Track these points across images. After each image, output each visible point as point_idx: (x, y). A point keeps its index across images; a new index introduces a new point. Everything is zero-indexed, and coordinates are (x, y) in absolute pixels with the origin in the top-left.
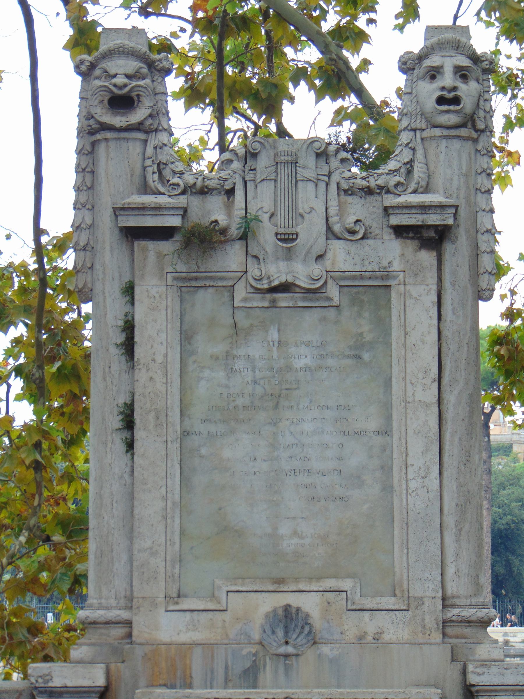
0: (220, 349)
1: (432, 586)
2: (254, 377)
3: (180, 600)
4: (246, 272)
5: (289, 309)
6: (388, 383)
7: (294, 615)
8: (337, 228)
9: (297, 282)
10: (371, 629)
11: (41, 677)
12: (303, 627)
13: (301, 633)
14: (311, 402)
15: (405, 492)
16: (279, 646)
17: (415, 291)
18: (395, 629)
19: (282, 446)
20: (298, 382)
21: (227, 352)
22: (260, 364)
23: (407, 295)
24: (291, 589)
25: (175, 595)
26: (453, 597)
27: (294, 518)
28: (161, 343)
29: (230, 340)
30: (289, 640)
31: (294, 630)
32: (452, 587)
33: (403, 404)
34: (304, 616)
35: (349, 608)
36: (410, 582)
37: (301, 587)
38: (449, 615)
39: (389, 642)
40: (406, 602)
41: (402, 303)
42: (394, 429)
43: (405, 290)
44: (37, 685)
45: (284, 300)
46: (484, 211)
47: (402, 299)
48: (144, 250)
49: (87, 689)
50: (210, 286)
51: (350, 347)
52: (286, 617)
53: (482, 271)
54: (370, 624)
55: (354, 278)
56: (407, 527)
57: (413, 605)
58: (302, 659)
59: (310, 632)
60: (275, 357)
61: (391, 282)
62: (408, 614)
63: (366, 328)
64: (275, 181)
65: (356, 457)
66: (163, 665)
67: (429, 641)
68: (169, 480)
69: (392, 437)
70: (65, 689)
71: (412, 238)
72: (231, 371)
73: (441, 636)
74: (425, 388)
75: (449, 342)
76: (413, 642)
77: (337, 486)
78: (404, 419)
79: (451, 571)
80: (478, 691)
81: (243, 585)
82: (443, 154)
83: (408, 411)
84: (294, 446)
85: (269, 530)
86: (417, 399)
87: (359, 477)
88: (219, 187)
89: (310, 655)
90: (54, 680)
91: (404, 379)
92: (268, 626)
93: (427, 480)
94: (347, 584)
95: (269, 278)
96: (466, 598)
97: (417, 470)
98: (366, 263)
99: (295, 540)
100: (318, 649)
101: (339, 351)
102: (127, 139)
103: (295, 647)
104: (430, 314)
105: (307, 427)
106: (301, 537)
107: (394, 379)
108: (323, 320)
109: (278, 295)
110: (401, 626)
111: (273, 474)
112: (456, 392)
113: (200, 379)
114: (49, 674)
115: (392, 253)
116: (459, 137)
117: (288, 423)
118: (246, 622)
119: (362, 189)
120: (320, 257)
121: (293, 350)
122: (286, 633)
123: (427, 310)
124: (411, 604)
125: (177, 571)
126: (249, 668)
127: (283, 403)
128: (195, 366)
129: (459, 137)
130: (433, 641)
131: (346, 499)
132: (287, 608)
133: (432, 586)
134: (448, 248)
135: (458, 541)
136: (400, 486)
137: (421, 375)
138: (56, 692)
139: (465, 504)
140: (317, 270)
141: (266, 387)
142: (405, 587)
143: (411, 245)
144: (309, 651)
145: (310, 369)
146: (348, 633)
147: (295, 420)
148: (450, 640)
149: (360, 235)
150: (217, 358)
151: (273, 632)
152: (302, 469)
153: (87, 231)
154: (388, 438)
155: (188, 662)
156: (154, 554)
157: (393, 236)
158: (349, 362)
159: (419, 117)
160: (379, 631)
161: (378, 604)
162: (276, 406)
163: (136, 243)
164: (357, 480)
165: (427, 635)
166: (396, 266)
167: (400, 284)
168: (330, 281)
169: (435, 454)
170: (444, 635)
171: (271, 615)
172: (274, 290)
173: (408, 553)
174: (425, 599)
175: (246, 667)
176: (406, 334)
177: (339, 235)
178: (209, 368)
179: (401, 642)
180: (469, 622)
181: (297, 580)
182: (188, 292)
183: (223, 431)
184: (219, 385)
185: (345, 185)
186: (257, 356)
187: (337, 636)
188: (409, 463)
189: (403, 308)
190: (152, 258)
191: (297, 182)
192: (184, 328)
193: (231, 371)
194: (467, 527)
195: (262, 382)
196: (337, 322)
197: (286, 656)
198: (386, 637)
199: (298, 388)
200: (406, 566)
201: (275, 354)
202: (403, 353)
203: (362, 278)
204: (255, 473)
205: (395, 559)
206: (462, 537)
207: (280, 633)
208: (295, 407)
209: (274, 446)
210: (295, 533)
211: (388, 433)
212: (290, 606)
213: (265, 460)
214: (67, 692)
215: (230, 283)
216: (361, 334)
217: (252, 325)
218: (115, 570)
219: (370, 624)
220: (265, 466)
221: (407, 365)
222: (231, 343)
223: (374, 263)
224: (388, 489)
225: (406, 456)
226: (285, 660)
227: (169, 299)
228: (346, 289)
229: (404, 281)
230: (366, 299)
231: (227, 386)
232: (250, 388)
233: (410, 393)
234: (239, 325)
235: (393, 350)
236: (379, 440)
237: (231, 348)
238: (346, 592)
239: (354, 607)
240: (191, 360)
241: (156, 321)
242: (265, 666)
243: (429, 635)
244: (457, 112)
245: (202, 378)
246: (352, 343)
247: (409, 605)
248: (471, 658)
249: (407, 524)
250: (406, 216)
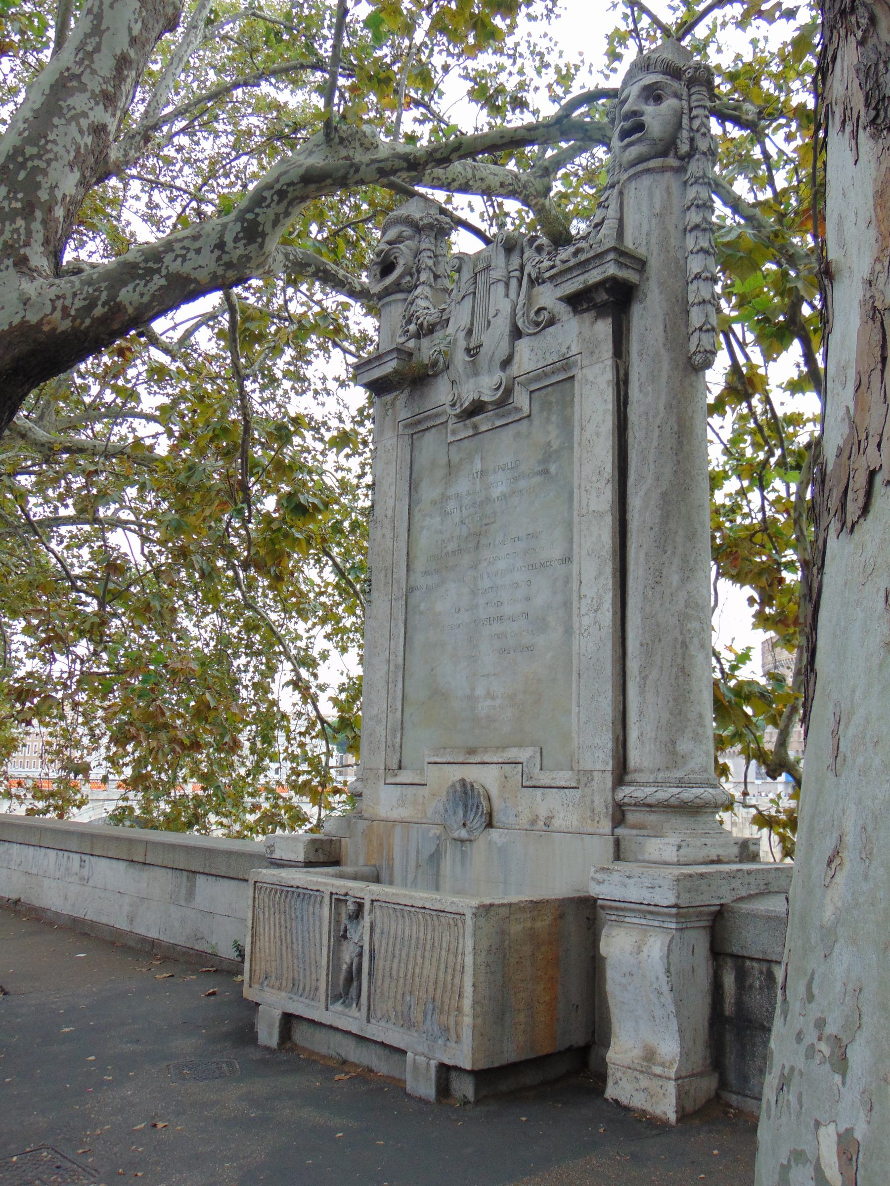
9: (482, 399)
20: (495, 513)
21: (443, 494)
25: (395, 767)
26: (635, 771)
45: (483, 421)
46: (692, 252)
53: (691, 330)
55: (538, 379)
57: (584, 780)
58: (475, 845)
62: (577, 793)
64: (474, 293)
67: (597, 831)
71: (588, 310)
72: (445, 514)
86: (591, 508)
87: (544, 619)
94: (524, 755)
96: (652, 772)
97: (589, 601)
99: (489, 702)
102: (389, 304)
103: (470, 832)
105: (502, 565)
106: (493, 698)
108: (517, 435)
109: (476, 419)
110: (571, 808)
112: (642, 493)
113: (422, 528)
116: (648, 171)
117: (485, 564)
120: (506, 363)
123: (602, 394)
125: (398, 740)
127: (484, 541)
129: (648, 171)
139: (653, 642)
145: (505, 496)
156: (379, 722)
158: (538, 479)
181: (486, 750)
193: (445, 514)
194: (654, 675)
195: (467, 521)
197: (462, 841)
198: (557, 823)
203: (546, 375)
206: (647, 689)
209: (473, 593)
216: (549, 444)
224: (568, 631)
246: (540, 457)
247: (579, 781)
250: (570, 282)
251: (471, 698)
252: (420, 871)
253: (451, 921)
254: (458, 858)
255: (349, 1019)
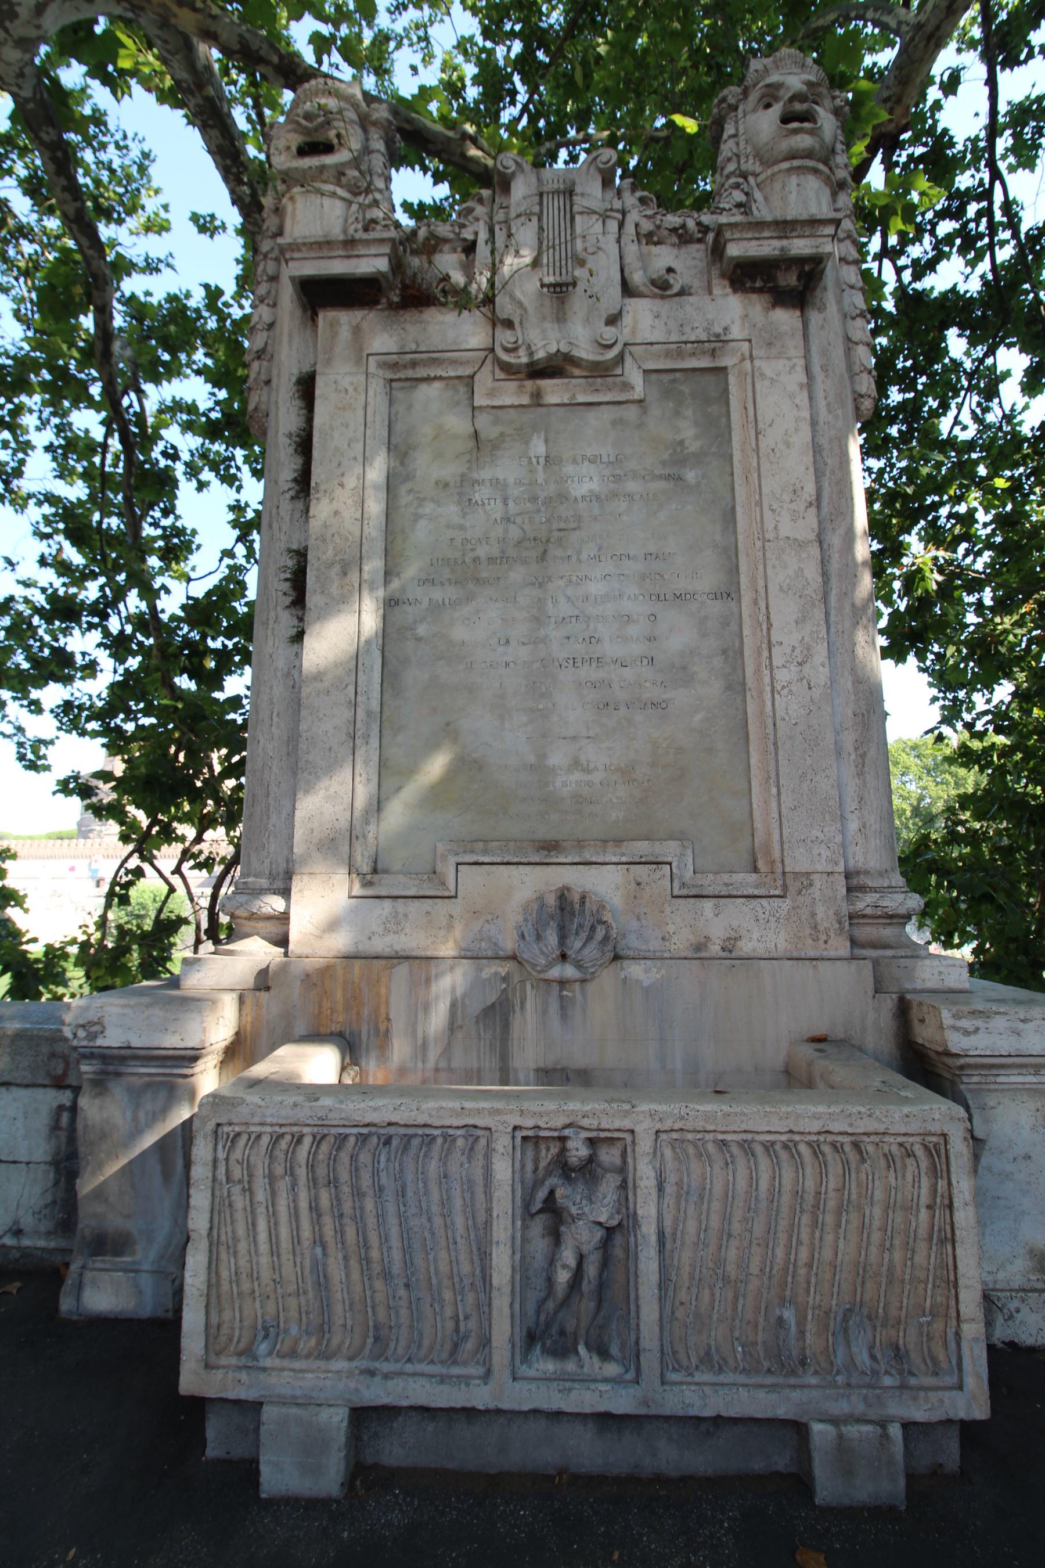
0: (450, 471)
1: (825, 853)
2: (507, 512)
3: (376, 878)
4: (492, 350)
5: (563, 409)
6: (730, 517)
7: (577, 906)
8: (637, 278)
10: (718, 932)
11: (83, 1026)
12: (593, 928)
13: (590, 938)
14: (600, 549)
15: (768, 689)
16: (550, 965)
17: (768, 368)
18: (760, 929)
19: (553, 620)
20: (579, 518)
22: (515, 492)
23: (757, 374)
24: (568, 860)
27: (574, 738)
28: (355, 458)
29: (467, 457)
30: (569, 953)
31: (577, 934)
32: (854, 854)
33: (759, 544)
34: (595, 908)
35: (676, 892)
36: (786, 846)
37: (588, 856)
38: (860, 905)
39: (752, 955)
40: (780, 883)
41: (750, 388)
42: (743, 587)
43: (753, 367)
44: (75, 1043)
45: (554, 391)
47: (749, 380)
48: (333, 325)
49: (171, 1052)
50: (435, 378)
51: (664, 463)
52: (562, 909)
54: (716, 922)
56: (776, 749)
57: (793, 886)
58: (591, 987)
59: (606, 938)
60: (540, 481)
61: (727, 361)
62: (785, 905)
63: (688, 431)
65: (679, 634)
66: (339, 995)
67: (825, 954)
68: (360, 674)
69: (739, 601)
70: (129, 1052)
71: (760, 291)
72: (468, 504)
73: (848, 944)
74: (795, 516)
75: (824, 454)
76: (795, 954)
77: (647, 684)
78: (761, 567)
79: (853, 826)
80: (962, 1067)
81: (485, 852)
82: (794, 194)
83: (768, 555)
84: (574, 620)
85: (532, 759)
87: (684, 668)
88: (452, 236)
89: (607, 979)
90: (107, 1033)
91: (760, 503)
92: (530, 926)
93: (806, 668)
94: (669, 850)
95: (529, 347)
97: (788, 651)
98: (687, 329)
99: (577, 776)
100: (622, 969)
101: (645, 469)
103: (579, 965)
104: (797, 401)
105: (595, 588)
106: (587, 771)
107: (739, 509)
109: (545, 383)
110: (773, 925)
111: (537, 665)
113: (417, 517)
114: (99, 1022)
115: (732, 312)
117: (561, 583)
118: (489, 917)
119: (674, 230)
120: (613, 320)
121: (569, 469)
122: (563, 938)
123: (792, 396)
124: (787, 884)
126: (493, 1004)
127: (554, 551)
128: (411, 497)
129: (816, 171)
130: (832, 954)
131: (664, 705)
132: (563, 895)
133: (825, 853)
134: (815, 317)
135: (860, 774)
136: (759, 679)
137: (786, 497)
138: (112, 1057)
140: (609, 333)
141: (525, 527)
142: (777, 854)
143: (757, 305)
144: (605, 972)
146: (675, 939)
147: (574, 578)
148: (866, 952)
149: (676, 289)
150: (447, 485)
151: (539, 937)
152: (587, 657)
153: (265, 334)
154: (733, 604)
155: (383, 991)
157: (729, 290)
158: (661, 485)
159: (751, 158)
160: (733, 934)
161: (726, 885)
162: (543, 557)
163: (321, 316)
164: (681, 673)
165: (821, 942)
166: (736, 332)
167: (743, 359)
168: (628, 360)
169: (818, 625)
170: (854, 943)
171: (535, 906)
172: (538, 371)
173: (779, 794)
174: (813, 877)
175: (489, 1004)
176: (757, 434)
177: (642, 288)
178: (432, 500)
179: (774, 955)
180: (891, 917)
181: (580, 844)
182: (402, 388)
183: (454, 598)
184: (448, 527)
185: (647, 226)
186: (511, 481)
187: (655, 945)
188: (774, 640)
189: (750, 394)
190: (345, 333)
191: (572, 219)
192: (393, 441)
193: (468, 504)
195: (519, 520)
196: (640, 426)
197: (563, 983)
199: (579, 528)
200: (776, 816)
201: (541, 477)
202: (755, 464)
204: (507, 665)
205: (754, 806)
207: (552, 938)
208: (574, 558)
209: (538, 620)
210: (576, 764)
211: (733, 595)
212: (568, 889)
213: (523, 644)
214: (135, 1058)
215: (468, 371)
216: (681, 443)
217: (502, 434)
218: (271, 827)
219: (716, 922)
220: (524, 653)
221: (763, 482)
222: (469, 461)
223: (700, 330)
225: (769, 630)
226: (561, 991)
227: (371, 393)
228: (654, 376)
229: (751, 356)
230: (687, 391)
231: (462, 527)
232: (499, 530)
233: (769, 525)
234: (483, 435)
235: (736, 463)
236: (716, 608)
237: (469, 469)
238: (670, 864)
239: (684, 892)
240: (403, 490)
241: (347, 426)
242: (523, 1003)
243: (826, 942)
244: (811, 132)
245: (421, 516)
246: (666, 456)
247: (785, 887)
248: (908, 986)
249: (775, 744)
250: (754, 243)
251: (540, 769)
252: (460, 1035)
253: (895, 1149)
254: (554, 1007)
255: (595, 1387)
